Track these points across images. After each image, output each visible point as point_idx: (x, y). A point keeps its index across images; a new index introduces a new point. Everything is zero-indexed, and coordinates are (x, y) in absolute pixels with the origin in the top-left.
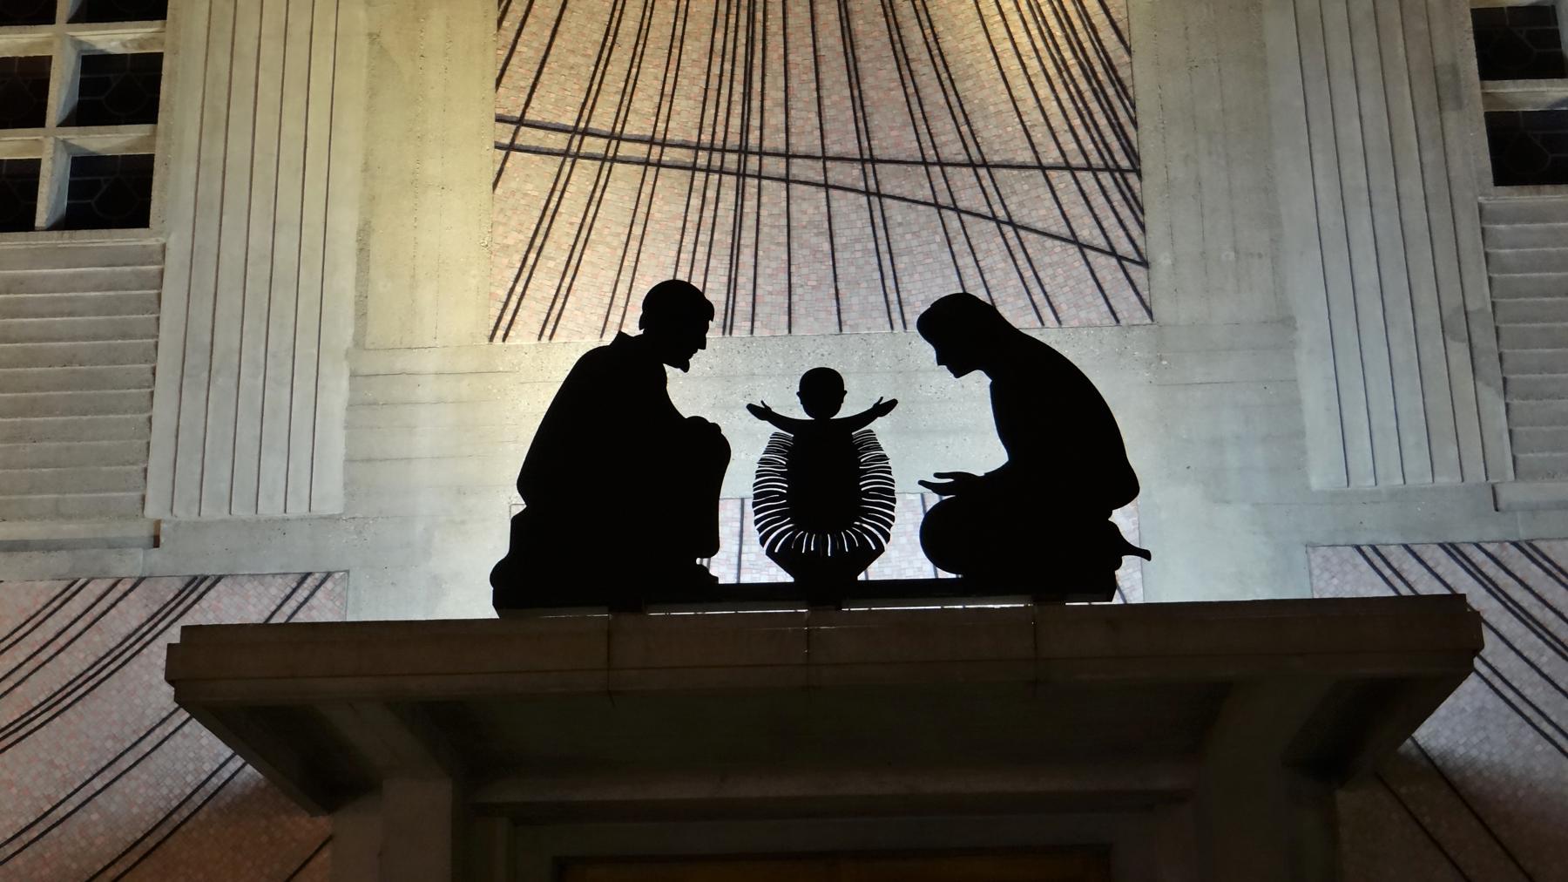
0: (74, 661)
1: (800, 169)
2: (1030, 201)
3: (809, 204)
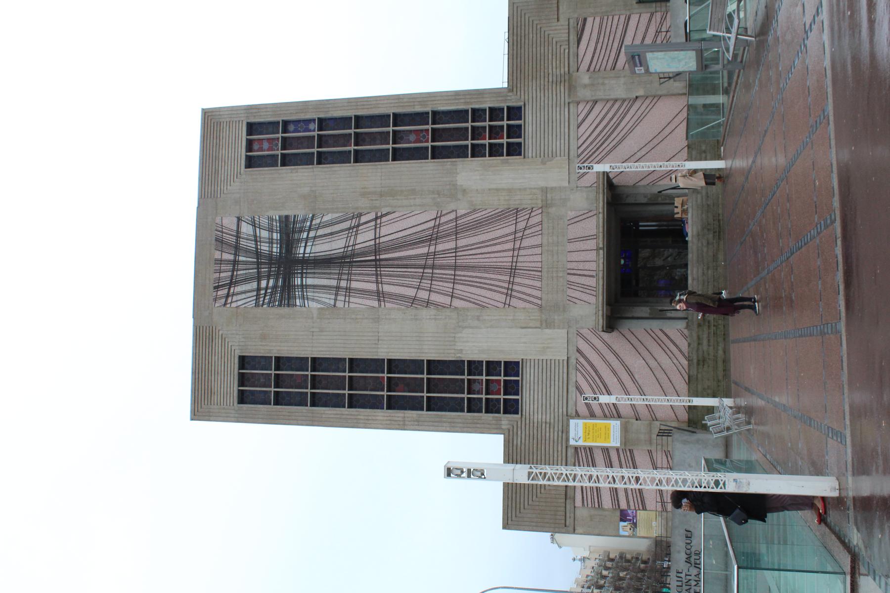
0: (589, 368)
1: (515, 260)
2: (521, 225)
3: (520, 259)
